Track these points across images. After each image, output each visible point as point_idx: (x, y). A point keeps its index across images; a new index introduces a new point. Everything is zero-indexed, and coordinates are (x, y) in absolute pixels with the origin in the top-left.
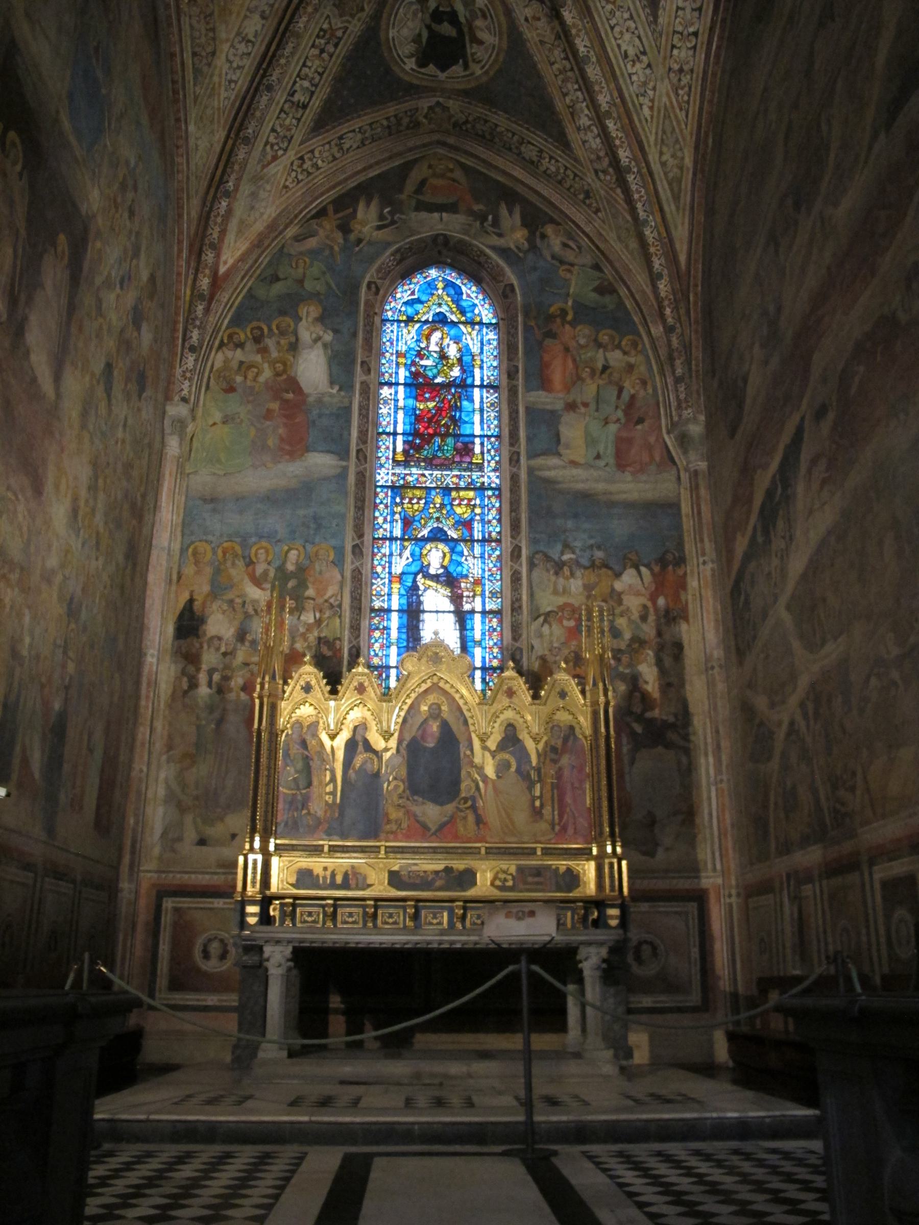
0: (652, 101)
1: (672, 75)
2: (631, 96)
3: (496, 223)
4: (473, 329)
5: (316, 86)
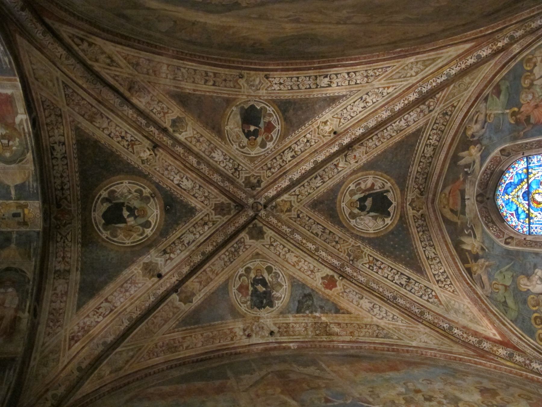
0: (384, 88)
1: (370, 81)
2: (383, 101)
3: (468, 166)
4: (531, 173)
5: (398, 272)
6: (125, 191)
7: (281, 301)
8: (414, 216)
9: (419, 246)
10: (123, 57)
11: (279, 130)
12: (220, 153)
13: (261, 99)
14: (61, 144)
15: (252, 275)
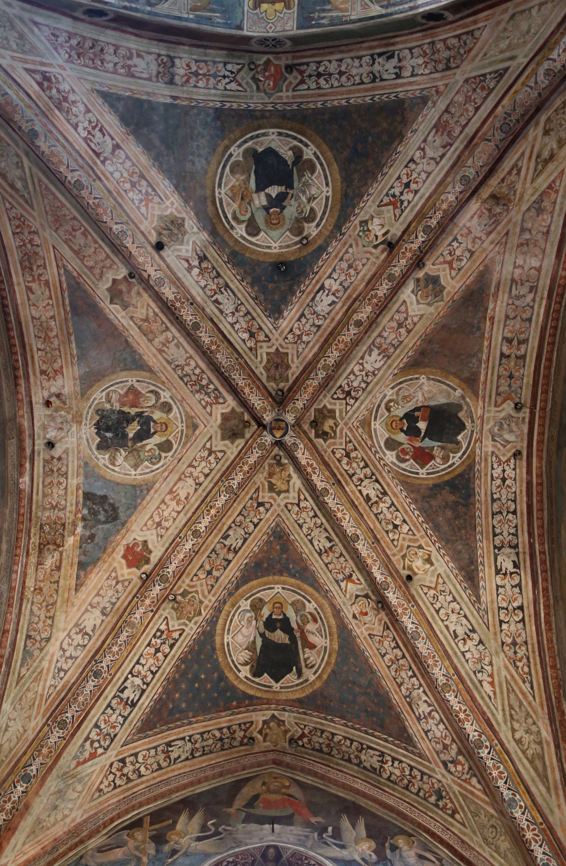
0: (491, 676)
3: (337, 834)
5: (148, 685)
6: (314, 191)
7: (107, 464)
8: (252, 723)
9: (194, 729)
10: (554, 181)
11: (417, 473)
12: (378, 365)
13: (476, 442)
14: (397, 70)
15: (157, 415)
